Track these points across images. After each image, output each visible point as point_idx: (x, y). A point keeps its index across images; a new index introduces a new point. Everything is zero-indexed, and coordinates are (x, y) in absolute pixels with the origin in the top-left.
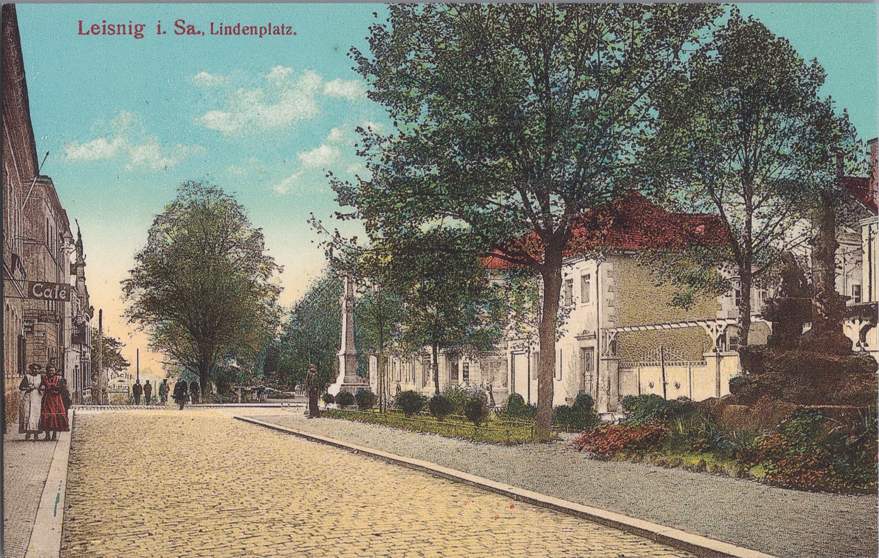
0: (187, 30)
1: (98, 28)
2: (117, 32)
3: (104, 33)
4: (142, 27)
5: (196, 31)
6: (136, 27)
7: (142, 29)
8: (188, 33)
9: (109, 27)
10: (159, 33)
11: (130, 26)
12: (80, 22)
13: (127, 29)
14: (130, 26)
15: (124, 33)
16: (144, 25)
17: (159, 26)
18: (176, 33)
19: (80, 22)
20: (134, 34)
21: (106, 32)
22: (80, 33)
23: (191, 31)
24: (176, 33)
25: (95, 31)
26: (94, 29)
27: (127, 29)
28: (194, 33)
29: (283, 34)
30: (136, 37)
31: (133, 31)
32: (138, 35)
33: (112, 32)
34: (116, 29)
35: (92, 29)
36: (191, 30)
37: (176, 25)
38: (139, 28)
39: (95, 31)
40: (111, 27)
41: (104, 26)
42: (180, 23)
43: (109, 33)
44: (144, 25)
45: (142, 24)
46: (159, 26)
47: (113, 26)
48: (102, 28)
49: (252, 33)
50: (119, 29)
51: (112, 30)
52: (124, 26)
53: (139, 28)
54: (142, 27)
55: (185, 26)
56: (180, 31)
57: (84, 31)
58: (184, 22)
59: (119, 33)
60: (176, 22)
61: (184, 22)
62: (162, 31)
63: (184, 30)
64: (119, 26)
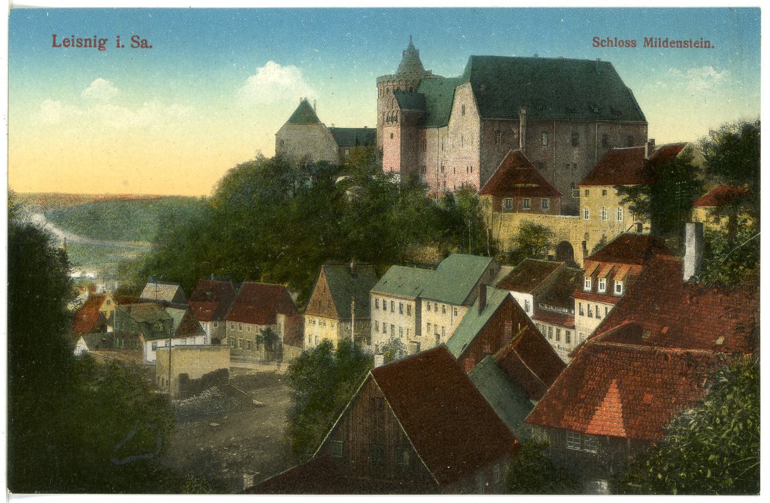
0: (141, 44)
1: (69, 41)
2: (84, 45)
3: (73, 46)
4: (105, 41)
5: (149, 45)
6: (100, 42)
7: (105, 43)
8: (142, 47)
9: (77, 41)
10: (118, 46)
11: (95, 40)
12: (54, 36)
13: (93, 44)
14: (95, 40)
15: (90, 46)
16: (107, 40)
17: (118, 41)
18: (132, 46)
19: (54, 36)
20: (98, 47)
21: (75, 46)
22: (54, 45)
23: (144, 46)
24: (132, 46)
25: (67, 44)
26: (66, 43)
27: (93, 44)
28: (147, 47)
29: (691, 47)
30: (99, 49)
31: (97, 44)
32: (101, 47)
33: (79, 45)
34: (84, 43)
35: (64, 42)
36: (145, 44)
37: (132, 39)
38: (102, 42)
39: (67, 44)
40: (80, 41)
41: (73, 40)
42: (135, 39)
43: (78, 46)
44: (107, 40)
45: (104, 38)
46: (118, 41)
47: (81, 40)
48: (71, 42)
49: (677, 47)
50: (86, 43)
51: (79, 43)
52: (90, 40)
53: (102, 42)
54: (105, 41)
55: (140, 41)
56: (135, 45)
57: (58, 43)
58: (138, 37)
59: (86, 46)
60: (133, 37)
61: (138, 37)
62: (121, 45)
63: (138, 43)
64: (86, 40)
